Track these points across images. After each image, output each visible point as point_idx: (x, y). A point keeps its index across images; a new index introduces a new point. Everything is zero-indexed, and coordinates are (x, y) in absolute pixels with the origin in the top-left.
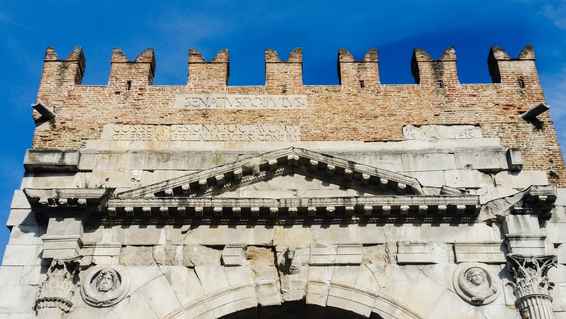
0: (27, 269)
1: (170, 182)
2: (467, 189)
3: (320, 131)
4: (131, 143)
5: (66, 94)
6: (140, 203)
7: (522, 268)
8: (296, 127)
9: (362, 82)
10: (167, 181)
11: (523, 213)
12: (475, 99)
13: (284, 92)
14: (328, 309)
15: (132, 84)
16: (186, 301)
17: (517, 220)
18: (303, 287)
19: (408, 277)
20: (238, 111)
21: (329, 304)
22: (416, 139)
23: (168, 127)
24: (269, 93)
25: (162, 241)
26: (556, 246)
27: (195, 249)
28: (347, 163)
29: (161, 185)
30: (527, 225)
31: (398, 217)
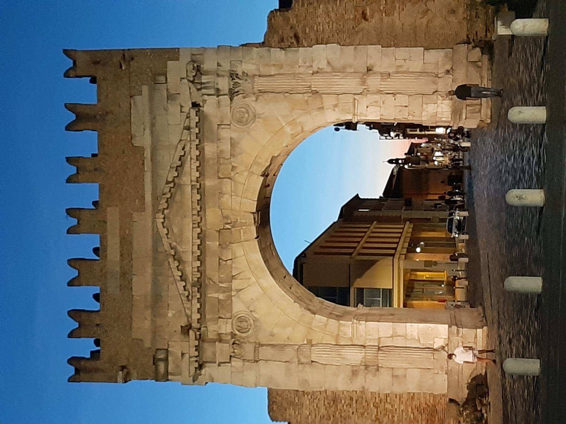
0: (234, 370)
1: (181, 292)
2: (181, 112)
3: (137, 200)
4: (146, 319)
5: (107, 365)
6: (195, 309)
7: (236, 90)
8: (134, 215)
9: (96, 170)
10: (180, 294)
11: (201, 83)
12: (109, 95)
13: (105, 222)
14: (258, 201)
15: (98, 323)
16: (253, 279)
17: (205, 88)
18: (245, 214)
19: (240, 154)
20: (120, 252)
21: (256, 199)
22: (144, 140)
23: (135, 297)
24: (106, 231)
25: (216, 295)
26: (219, 65)
27: (222, 276)
28: (167, 185)
29: (183, 298)
30: (208, 83)
31: (201, 158)
